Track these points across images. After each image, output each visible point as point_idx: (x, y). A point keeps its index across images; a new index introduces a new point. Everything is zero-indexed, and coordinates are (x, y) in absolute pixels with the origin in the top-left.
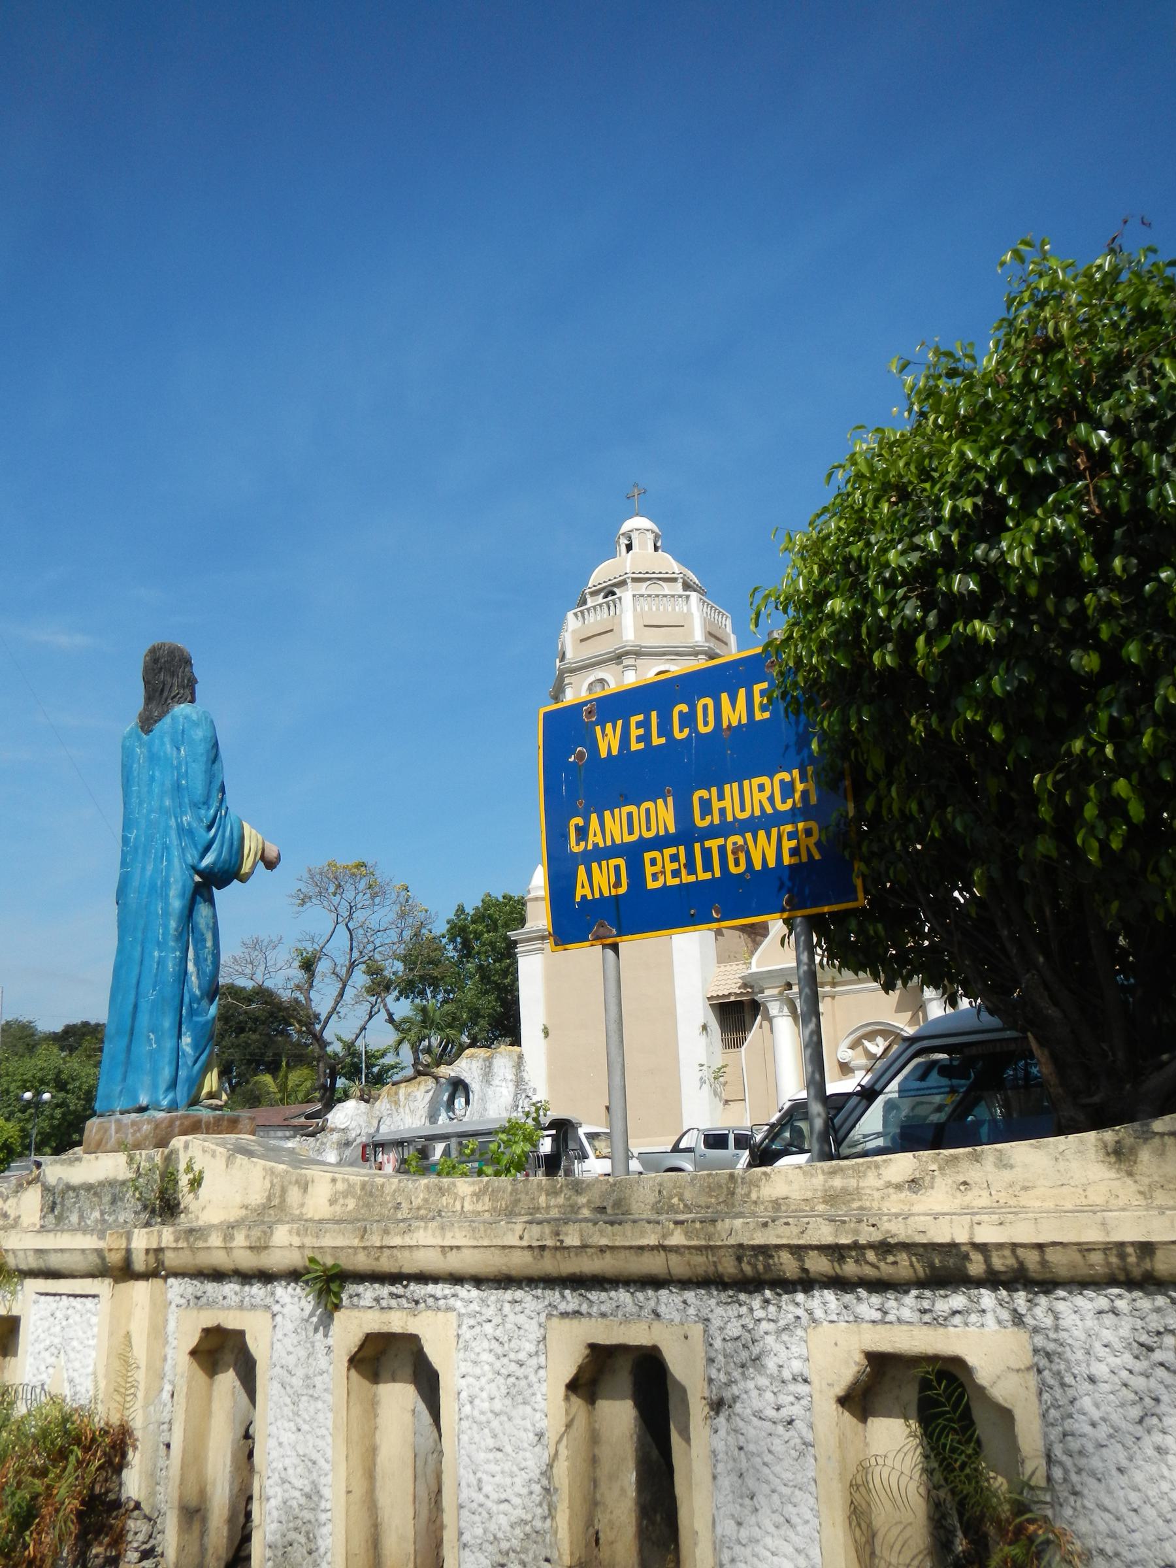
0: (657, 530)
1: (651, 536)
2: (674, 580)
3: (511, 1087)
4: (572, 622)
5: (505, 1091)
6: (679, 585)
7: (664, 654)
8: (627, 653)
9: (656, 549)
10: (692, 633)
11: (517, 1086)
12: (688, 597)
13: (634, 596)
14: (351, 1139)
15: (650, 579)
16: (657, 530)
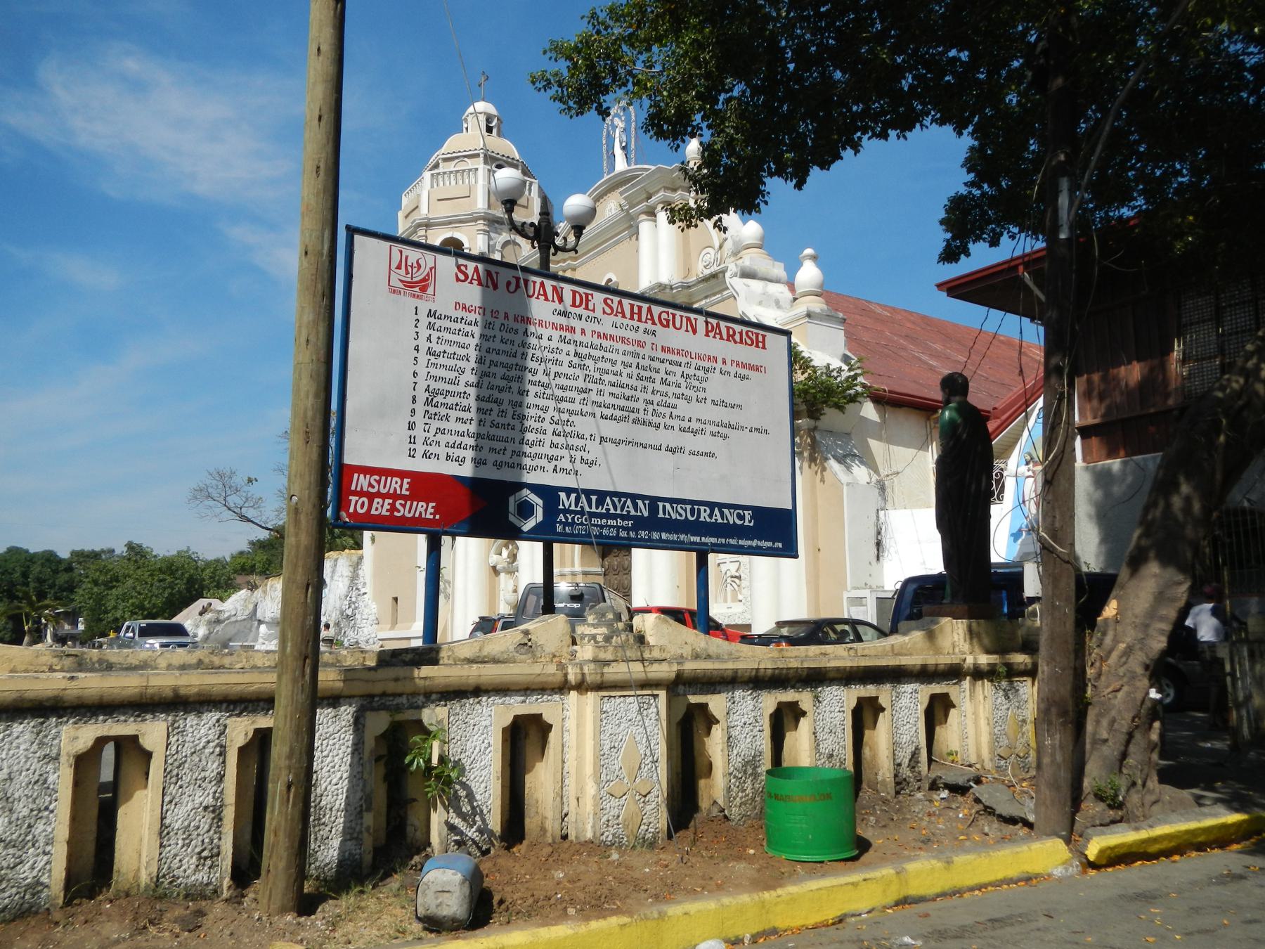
0: (492, 109)
1: (482, 118)
2: (477, 156)
3: (347, 582)
4: (405, 201)
5: (341, 585)
6: (481, 159)
7: (450, 223)
8: (419, 225)
9: (489, 130)
10: (476, 202)
11: (352, 581)
12: (477, 169)
13: (432, 175)
14: (221, 618)
15: (457, 158)
16: (492, 109)
